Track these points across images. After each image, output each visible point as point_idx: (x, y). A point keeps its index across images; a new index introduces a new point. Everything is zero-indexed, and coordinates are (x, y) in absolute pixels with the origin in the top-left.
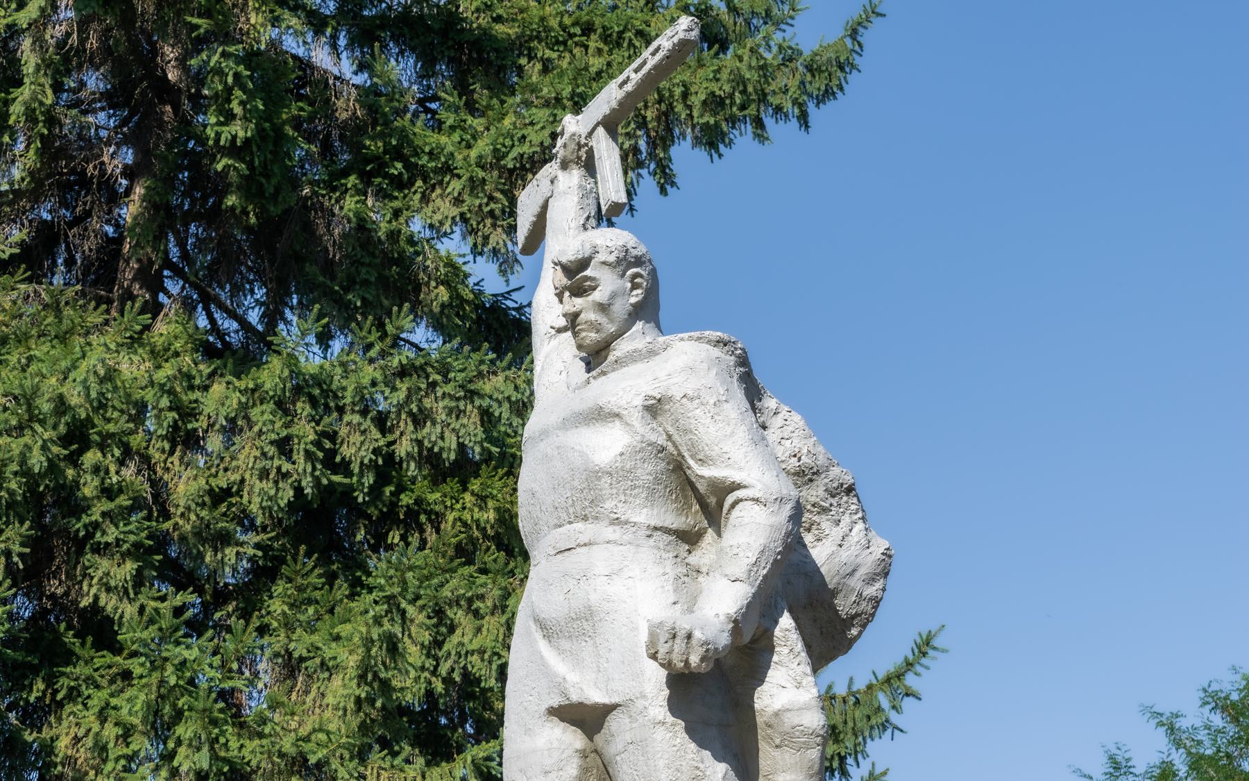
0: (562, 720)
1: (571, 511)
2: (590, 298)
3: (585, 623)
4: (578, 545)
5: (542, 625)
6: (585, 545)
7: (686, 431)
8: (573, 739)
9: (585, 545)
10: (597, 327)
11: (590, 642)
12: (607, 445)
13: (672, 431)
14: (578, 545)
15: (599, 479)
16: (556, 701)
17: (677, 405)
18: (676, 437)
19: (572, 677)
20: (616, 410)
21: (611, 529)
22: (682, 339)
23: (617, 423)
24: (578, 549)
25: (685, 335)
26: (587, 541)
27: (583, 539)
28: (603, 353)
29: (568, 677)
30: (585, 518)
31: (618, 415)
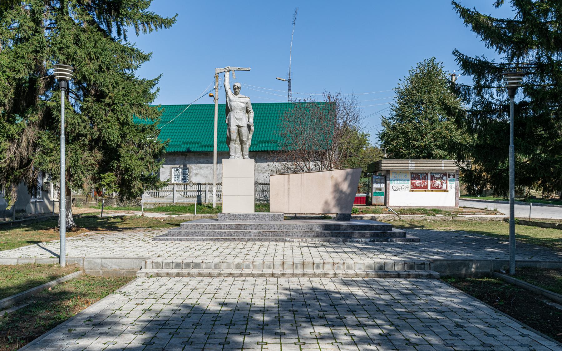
8: (237, 128)
12: (243, 105)
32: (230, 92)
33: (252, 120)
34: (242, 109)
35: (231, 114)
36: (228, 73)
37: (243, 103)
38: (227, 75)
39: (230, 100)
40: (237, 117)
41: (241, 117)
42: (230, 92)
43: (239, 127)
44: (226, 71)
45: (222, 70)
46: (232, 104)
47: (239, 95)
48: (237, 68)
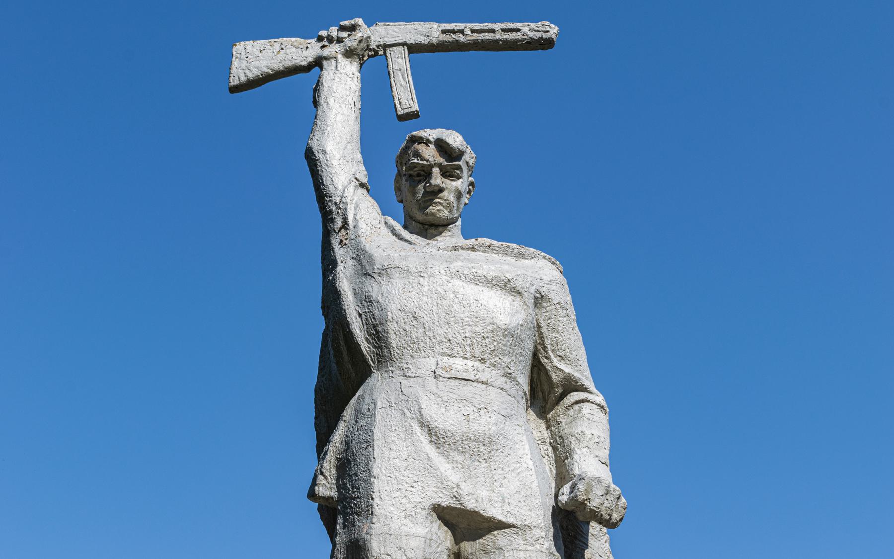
0: (439, 518)
1: (468, 349)
2: (454, 184)
3: (482, 448)
4: (477, 381)
5: (432, 432)
6: (482, 383)
7: (554, 330)
8: (444, 538)
9: (482, 383)
10: (449, 206)
11: (484, 465)
12: (506, 311)
13: (543, 324)
14: (477, 381)
15: (505, 336)
16: (445, 501)
17: (553, 307)
18: (544, 330)
19: (465, 488)
20: (519, 288)
21: (504, 379)
22: (545, 258)
23: (518, 299)
24: (476, 384)
25: (548, 256)
26: (484, 380)
27: (483, 377)
28: (441, 229)
29: (463, 485)
30: (482, 361)
31: (519, 293)
32: (368, 221)
33: (592, 463)
34: (490, 344)
35: (379, 390)
36: (351, 68)
37: (508, 287)
38: (342, 84)
39: (366, 268)
40: (447, 419)
41: (485, 424)
42: (368, 221)
43: (464, 524)
44: (333, 49)
45: (296, 51)
46: (397, 298)
47: (452, 237)
48: (429, 31)
